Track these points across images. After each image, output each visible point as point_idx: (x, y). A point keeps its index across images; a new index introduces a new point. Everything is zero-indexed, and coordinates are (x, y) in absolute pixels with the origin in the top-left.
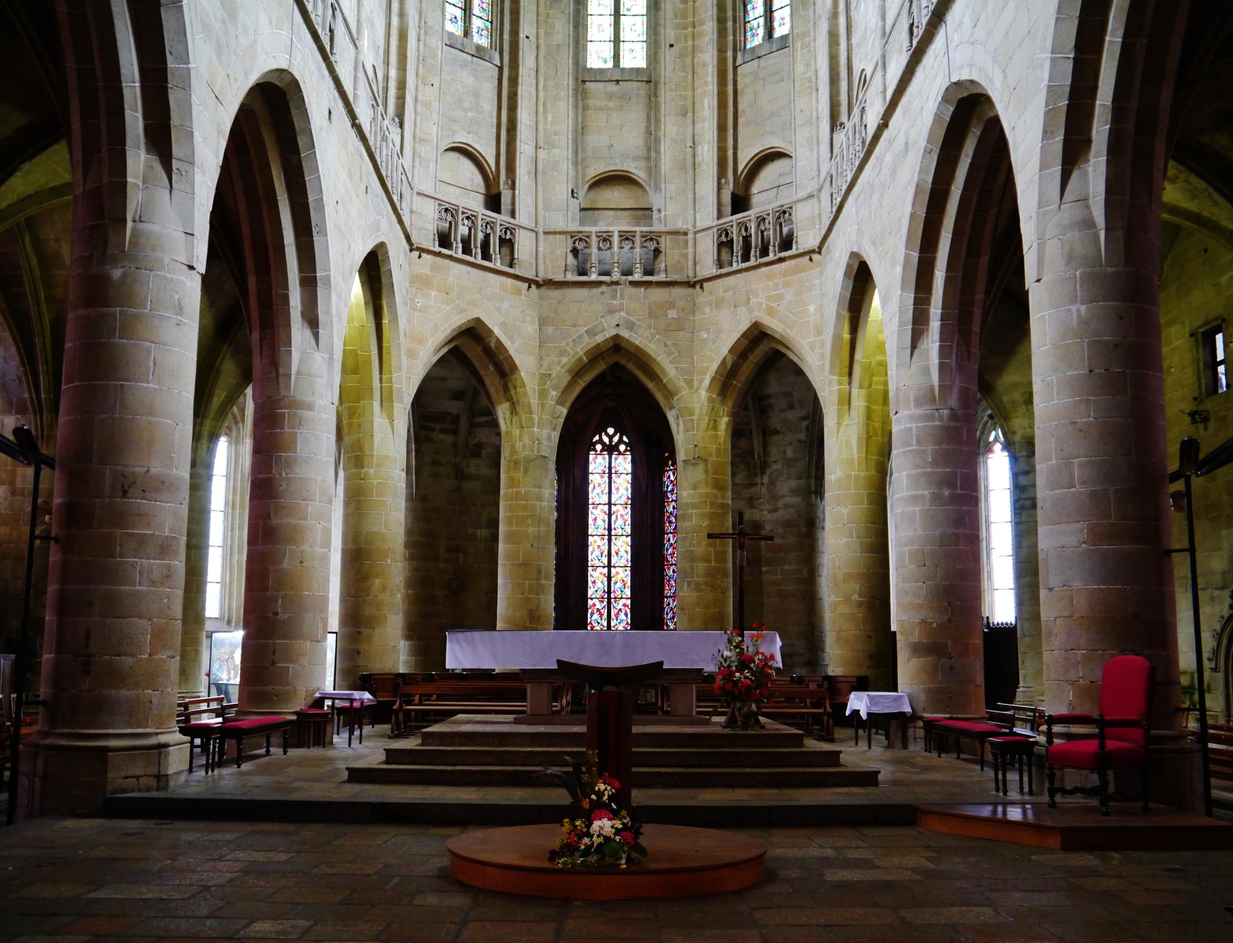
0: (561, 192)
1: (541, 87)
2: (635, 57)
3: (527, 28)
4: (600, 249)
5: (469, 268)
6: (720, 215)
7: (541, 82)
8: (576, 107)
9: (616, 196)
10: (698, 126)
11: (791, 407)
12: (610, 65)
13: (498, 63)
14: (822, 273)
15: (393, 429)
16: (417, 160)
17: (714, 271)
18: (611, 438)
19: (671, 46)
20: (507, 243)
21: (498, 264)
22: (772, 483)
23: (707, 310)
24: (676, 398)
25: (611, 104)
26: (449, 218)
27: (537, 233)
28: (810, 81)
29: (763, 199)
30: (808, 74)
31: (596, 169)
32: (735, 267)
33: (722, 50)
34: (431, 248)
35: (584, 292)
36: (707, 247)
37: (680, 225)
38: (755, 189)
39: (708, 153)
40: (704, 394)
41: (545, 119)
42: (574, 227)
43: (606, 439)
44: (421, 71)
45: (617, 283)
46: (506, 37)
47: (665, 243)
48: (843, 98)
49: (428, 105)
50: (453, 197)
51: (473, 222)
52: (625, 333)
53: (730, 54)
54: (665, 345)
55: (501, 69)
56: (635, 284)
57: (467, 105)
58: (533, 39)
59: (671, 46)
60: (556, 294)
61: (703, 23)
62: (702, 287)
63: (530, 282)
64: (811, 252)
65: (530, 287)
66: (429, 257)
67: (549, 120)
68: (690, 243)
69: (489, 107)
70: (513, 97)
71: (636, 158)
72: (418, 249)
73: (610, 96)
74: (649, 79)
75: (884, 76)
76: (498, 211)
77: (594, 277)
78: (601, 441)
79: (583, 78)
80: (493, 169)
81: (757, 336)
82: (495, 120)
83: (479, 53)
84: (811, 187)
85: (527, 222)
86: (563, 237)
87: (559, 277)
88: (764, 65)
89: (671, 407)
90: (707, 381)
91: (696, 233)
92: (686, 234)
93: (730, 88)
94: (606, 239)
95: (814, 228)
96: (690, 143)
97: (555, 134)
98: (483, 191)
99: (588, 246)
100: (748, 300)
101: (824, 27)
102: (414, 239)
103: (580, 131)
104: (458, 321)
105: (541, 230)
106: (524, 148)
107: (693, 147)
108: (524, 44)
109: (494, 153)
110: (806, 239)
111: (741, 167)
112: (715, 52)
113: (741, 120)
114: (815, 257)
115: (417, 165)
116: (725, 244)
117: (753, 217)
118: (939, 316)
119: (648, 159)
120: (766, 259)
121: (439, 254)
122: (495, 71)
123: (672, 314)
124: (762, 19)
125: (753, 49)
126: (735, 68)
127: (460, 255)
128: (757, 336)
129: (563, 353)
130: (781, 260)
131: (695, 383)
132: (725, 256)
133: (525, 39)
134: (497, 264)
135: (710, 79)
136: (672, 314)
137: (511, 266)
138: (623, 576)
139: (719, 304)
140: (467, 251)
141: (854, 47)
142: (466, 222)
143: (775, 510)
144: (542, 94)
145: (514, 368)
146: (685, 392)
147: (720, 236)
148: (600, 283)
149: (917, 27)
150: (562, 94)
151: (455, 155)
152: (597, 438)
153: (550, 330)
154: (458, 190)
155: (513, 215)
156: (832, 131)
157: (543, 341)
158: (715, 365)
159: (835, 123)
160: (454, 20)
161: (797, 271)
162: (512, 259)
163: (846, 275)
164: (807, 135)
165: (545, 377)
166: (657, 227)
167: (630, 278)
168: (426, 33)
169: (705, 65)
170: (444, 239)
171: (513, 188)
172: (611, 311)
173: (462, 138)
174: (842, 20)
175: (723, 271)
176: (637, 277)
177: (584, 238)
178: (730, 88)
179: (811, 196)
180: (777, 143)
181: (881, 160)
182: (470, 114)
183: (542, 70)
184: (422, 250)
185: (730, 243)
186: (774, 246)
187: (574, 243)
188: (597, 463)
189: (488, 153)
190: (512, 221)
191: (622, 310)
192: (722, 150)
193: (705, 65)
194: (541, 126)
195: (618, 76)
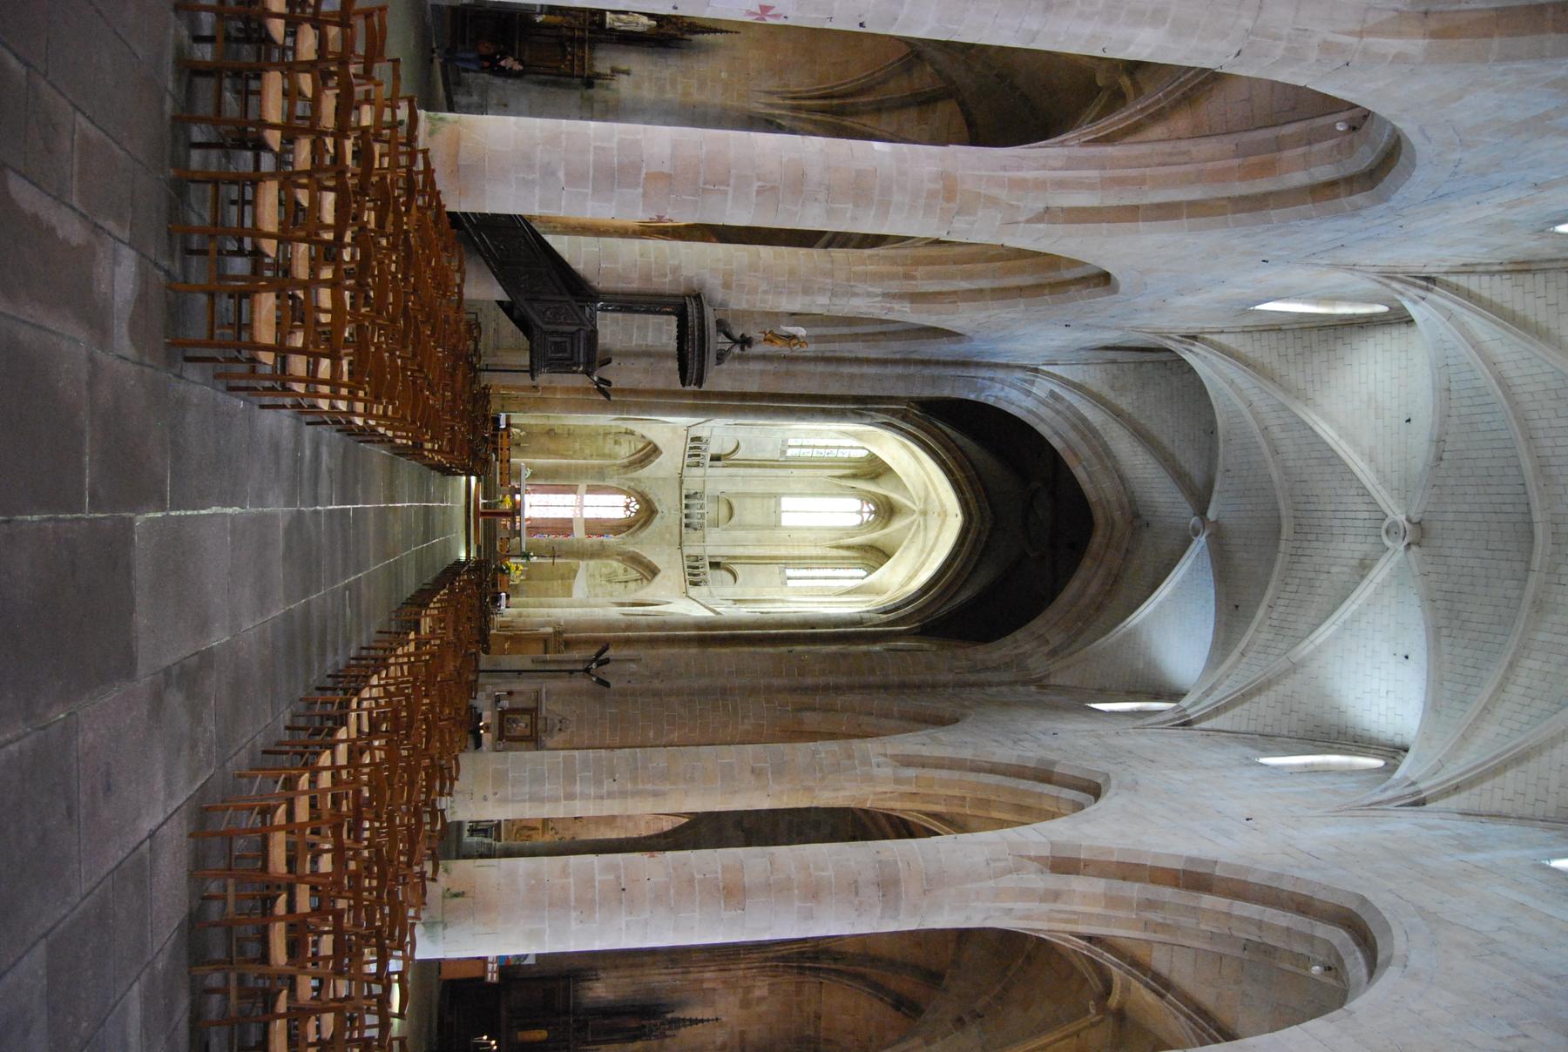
0: (723, 487)
6: (710, 557)
9: (724, 510)
20: (698, 465)
29: (711, 574)
33: (786, 558)
37: (707, 539)
38: (724, 573)
39: (739, 551)
40: (632, 549)
43: (632, 504)
47: (699, 533)
50: (712, 441)
52: (658, 516)
60: (677, 486)
69: (760, 456)
74: (777, 525)
77: (684, 502)
83: (784, 452)
87: (684, 486)
94: (702, 507)
98: (723, 453)
103: (752, 496)
104: (660, 445)
106: (741, 471)
110: (693, 591)
116: (697, 559)
127: (688, 446)
134: (686, 462)
136: (668, 536)
140: (691, 448)
145: (642, 467)
152: (633, 499)
157: (657, 479)
158: (644, 554)
165: (639, 480)
166: (706, 529)
170: (698, 439)
173: (742, 444)
176: (684, 520)
177: (701, 497)
180: (740, 580)
188: (621, 499)
195: (777, 513)
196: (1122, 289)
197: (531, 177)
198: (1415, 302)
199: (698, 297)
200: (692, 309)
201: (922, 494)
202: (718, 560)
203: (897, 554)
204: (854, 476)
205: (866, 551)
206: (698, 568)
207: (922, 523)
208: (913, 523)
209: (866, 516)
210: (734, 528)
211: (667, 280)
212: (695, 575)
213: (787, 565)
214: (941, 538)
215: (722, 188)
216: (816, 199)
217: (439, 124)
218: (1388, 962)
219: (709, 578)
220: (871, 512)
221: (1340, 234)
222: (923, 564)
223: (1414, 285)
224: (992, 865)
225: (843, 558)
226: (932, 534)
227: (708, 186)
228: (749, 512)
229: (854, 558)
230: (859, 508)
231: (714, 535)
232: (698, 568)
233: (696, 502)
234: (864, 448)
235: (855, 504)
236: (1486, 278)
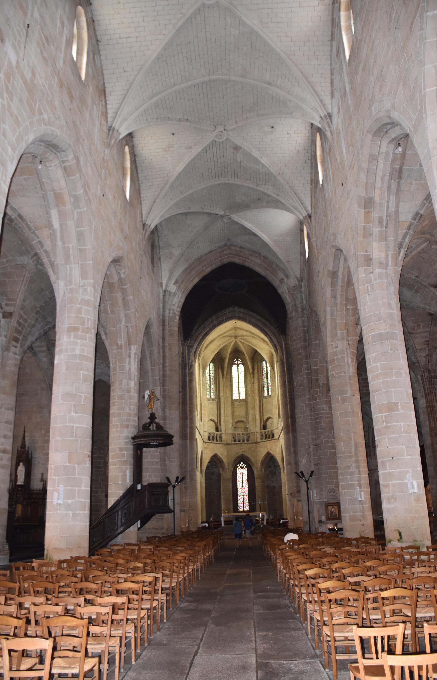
0: (230, 426)
2: (243, 396)
3: (222, 394)
6: (261, 430)
9: (240, 425)
12: (238, 398)
20: (221, 437)
25: (239, 406)
31: (236, 420)
32: (264, 440)
33: (259, 396)
35: (236, 445)
36: (259, 436)
37: (253, 431)
38: (267, 423)
39: (258, 417)
40: (259, 464)
42: (232, 432)
43: (241, 465)
47: (251, 435)
50: (210, 431)
52: (244, 453)
55: (217, 402)
56: (245, 443)
60: (230, 446)
63: (225, 444)
69: (215, 410)
73: (238, 405)
77: (237, 442)
79: (233, 401)
81: (268, 454)
87: (230, 443)
92: (254, 433)
93: (261, 404)
94: (239, 434)
102: (204, 440)
103: (233, 413)
104: (212, 454)
106: (223, 418)
107: (255, 416)
110: (276, 436)
113: (264, 410)
116: (262, 435)
119: (246, 417)
123: (253, 449)
127: (212, 442)
128: (268, 454)
134: (219, 442)
136: (253, 449)
137: (221, 441)
138: (246, 498)
139: (261, 447)
140: (213, 441)
145: (223, 462)
146: (256, 464)
148: (238, 444)
155: (221, 431)
158: (261, 459)
161: (275, 442)
165: (229, 463)
166: (249, 432)
170: (209, 438)
171: (221, 426)
172: (241, 449)
173: (211, 418)
176: (245, 442)
177: (235, 435)
178: (261, 404)
180: (270, 416)
185: (263, 435)
188: (239, 471)
189: (216, 420)
195: (239, 400)
196: (121, 255)
197: (71, 515)
198: (120, 134)
199: (133, 438)
200: (139, 441)
201: (227, 338)
204: (222, 369)
205: (255, 361)
206: (266, 435)
207: (240, 338)
208: (241, 342)
209: (239, 362)
210: (247, 419)
211: (125, 453)
212: (269, 436)
213: (263, 396)
214: (246, 329)
215: (74, 429)
216: (79, 387)
217: (48, 557)
218: (389, 117)
219: (270, 429)
220: (238, 360)
221: (88, 164)
222: (258, 336)
223: (112, 134)
224: (370, 293)
225: (258, 371)
226: (245, 333)
227: (74, 435)
228: (240, 413)
229: (258, 366)
230: (236, 366)
231: (252, 428)
232: (266, 435)
233: (237, 437)
234: (210, 365)
235: (234, 368)
236: (108, 107)
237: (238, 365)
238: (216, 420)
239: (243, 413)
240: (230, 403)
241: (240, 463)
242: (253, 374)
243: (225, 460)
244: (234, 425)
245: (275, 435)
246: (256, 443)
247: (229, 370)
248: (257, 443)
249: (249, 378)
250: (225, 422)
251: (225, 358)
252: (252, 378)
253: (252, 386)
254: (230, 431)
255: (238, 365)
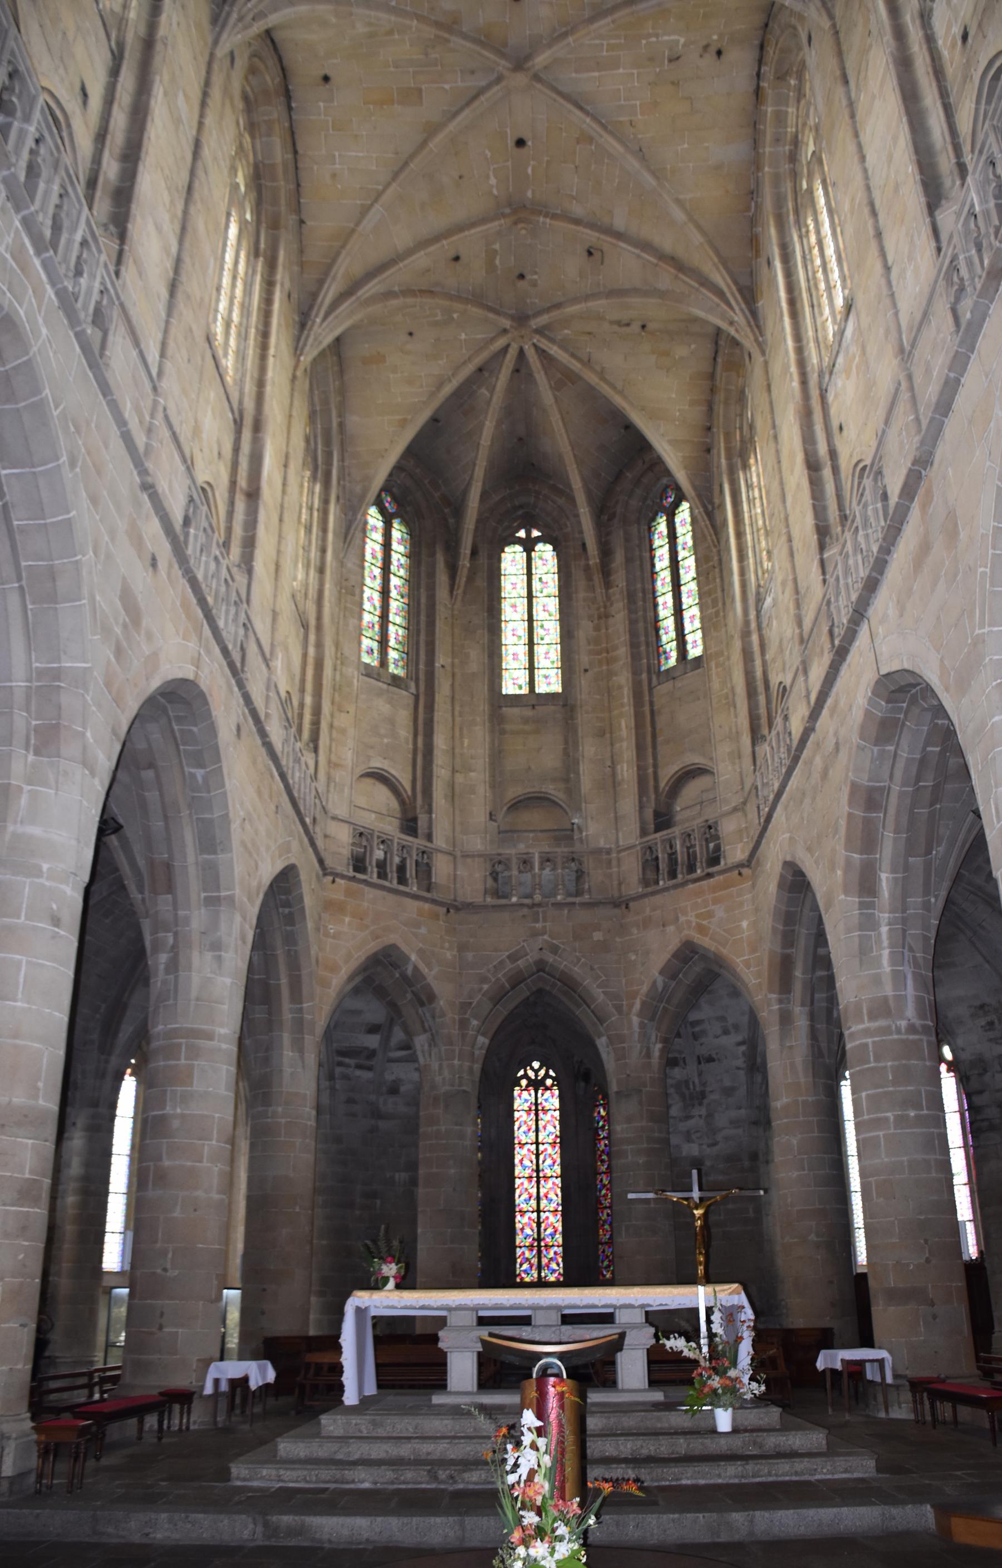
0: (479, 814)
1: (457, 713)
2: (549, 682)
3: (442, 659)
4: (520, 872)
5: (385, 893)
6: (644, 832)
7: (457, 708)
8: (492, 731)
9: (534, 818)
10: (617, 745)
11: (726, 1032)
12: (525, 691)
13: (413, 690)
14: (753, 886)
15: (303, 1062)
16: (332, 785)
17: (640, 890)
18: (536, 1072)
19: (586, 671)
20: (424, 871)
21: (415, 889)
22: (710, 1115)
23: (635, 931)
24: (605, 1025)
25: (527, 728)
26: (364, 843)
27: (455, 857)
28: (727, 698)
30: (725, 691)
31: (513, 792)
33: (636, 672)
34: (345, 873)
36: (631, 867)
37: (602, 843)
39: (627, 772)
41: (462, 743)
43: (531, 1074)
44: (337, 698)
45: (539, 905)
46: (422, 667)
48: (763, 711)
49: (343, 731)
50: (368, 820)
51: (388, 846)
52: (550, 958)
53: (644, 676)
54: (592, 969)
55: (417, 697)
56: (558, 905)
57: (382, 731)
58: (449, 668)
59: (586, 671)
61: (615, 648)
62: (627, 907)
64: (741, 865)
65: (448, 911)
66: (342, 882)
67: (466, 744)
68: (614, 863)
69: (404, 733)
70: (429, 723)
71: (554, 780)
72: (331, 874)
73: (526, 721)
75: (806, 681)
76: (416, 837)
78: (526, 1076)
79: (499, 701)
80: (410, 793)
82: (411, 746)
83: (395, 680)
84: (735, 801)
85: (444, 846)
86: (482, 859)
87: (479, 899)
88: (680, 685)
89: (600, 1036)
90: (637, 1006)
91: (619, 852)
92: (609, 852)
93: (647, 709)
95: (741, 841)
96: (609, 763)
97: (472, 758)
99: (508, 868)
100: (677, 919)
101: (737, 644)
102: (329, 862)
103: (497, 757)
104: (372, 947)
105: (458, 854)
106: (441, 772)
107: (613, 767)
108: (439, 673)
109: (411, 778)
110: (736, 852)
111: (662, 785)
112: (630, 675)
114: (745, 871)
115: (332, 789)
116: (650, 864)
117: (677, 833)
118: (886, 921)
119: (567, 780)
120: (694, 876)
121: (353, 879)
122: (411, 701)
123: (598, 936)
124: (675, 643)
125: (668, 671)
126: (651, 689)
129: (484, 980)
130: (709, 875)
131: (625, 1008)
132: (651, 875)
133: (441, 669)
135: (626, 700)
136: (598, 936)
137: (428, 890)
139: (646, 924)
140: (382, 875)
141: (769, 662)
142: (382, 847)
143: (715, 1144)
144: (458, 719)
145: (432, 997)
147: (645, 854)
149: (838, 627)
150: (478, 719)
151: (369, 781)
152: (521, 1073)
153: (470, 956)
154: (373, 816)
155: (429, 837)
156: (754, 744)
158: (645, 989)
159: (756, 736)
160: (370, 651)
161: (726, 886)
162: (430, 884)
163: (780, 886)
164: (728, 750)
166: (578, 847)
167: (552, 900)
168: (342, 663)
169: (620, 687)
170: (359, 864)
171: (430, 812)
172: (535, 934)
173: (377, 763)
174: (755, 638)
175: (650, 889)
179: (735, 810)
180: (696, 759)
181: (810, 762)
182: (386, 740)
183: (457, 697)
184: (336, 875)
186: (701, 862)
187: (493, 866)
188: (522, 1099)
189: (405, 780)
190: (429, 844)
191: (545, 933)
192: (641, 769)
193: (620, 687)
194: (457, 751)
195: (533, 699)
202: (649, 814)
203: (618, 400)
204: (452, 549)
206: (672, 858)
213: (656, 673)
225: (629, 560)
229: (627, 540)
230: (518, 548)
232: (672, 858)
235: (512, 558)
237: (529, 546)
238: (405, 780)
239: (550, 759)
240: (483, 707)
241: (527, 1063)
242: (606, 571)
243: (445, 993)
244: (500, 816)
245: (726, 848)
246: (616, 904)
247: (483, 560)
248: (623, 904)
249: (581, 594)
250: (452, 795)
251: (465, 492)
252: (600, 590)
253: (597, 629)
254: (477, 844)
255: (529, 546)
